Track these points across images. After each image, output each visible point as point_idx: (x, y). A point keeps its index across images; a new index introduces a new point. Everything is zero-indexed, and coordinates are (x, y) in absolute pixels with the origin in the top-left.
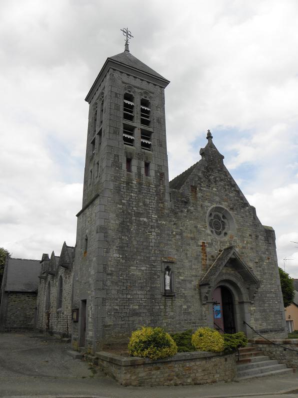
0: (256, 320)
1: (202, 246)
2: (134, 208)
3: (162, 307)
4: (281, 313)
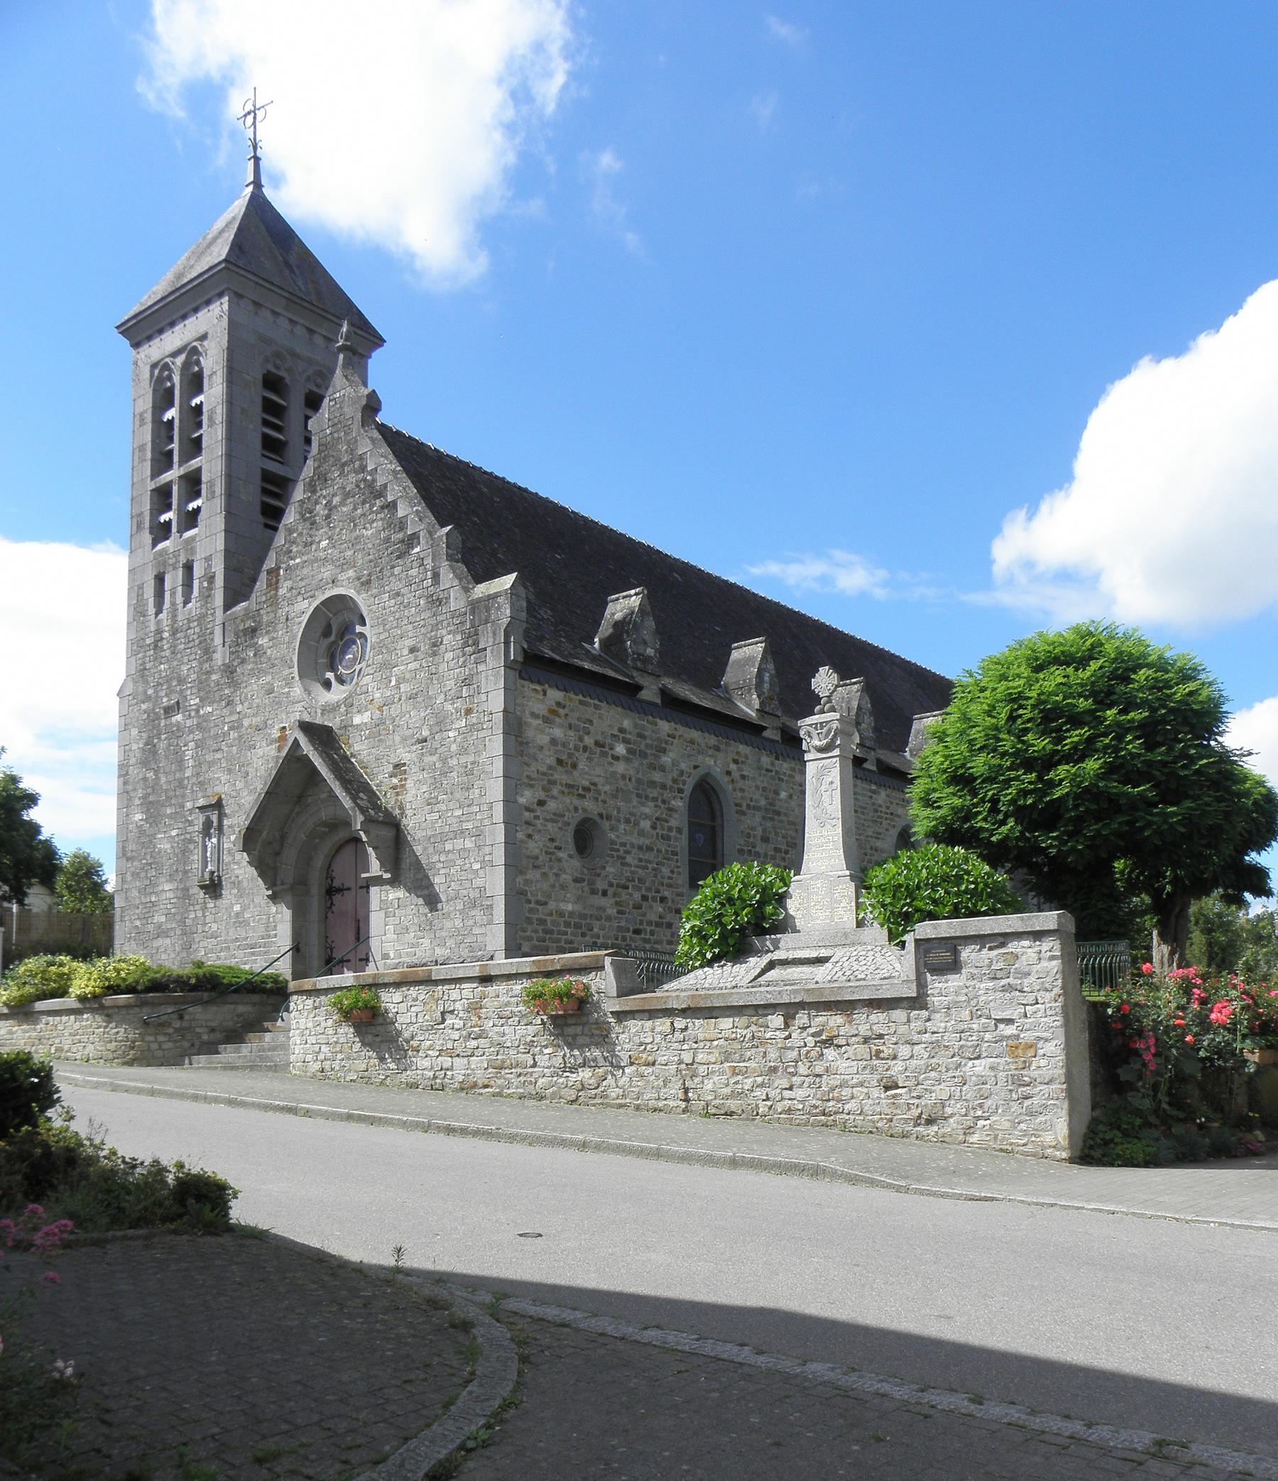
0: (402, 930)
3: (200, 914)
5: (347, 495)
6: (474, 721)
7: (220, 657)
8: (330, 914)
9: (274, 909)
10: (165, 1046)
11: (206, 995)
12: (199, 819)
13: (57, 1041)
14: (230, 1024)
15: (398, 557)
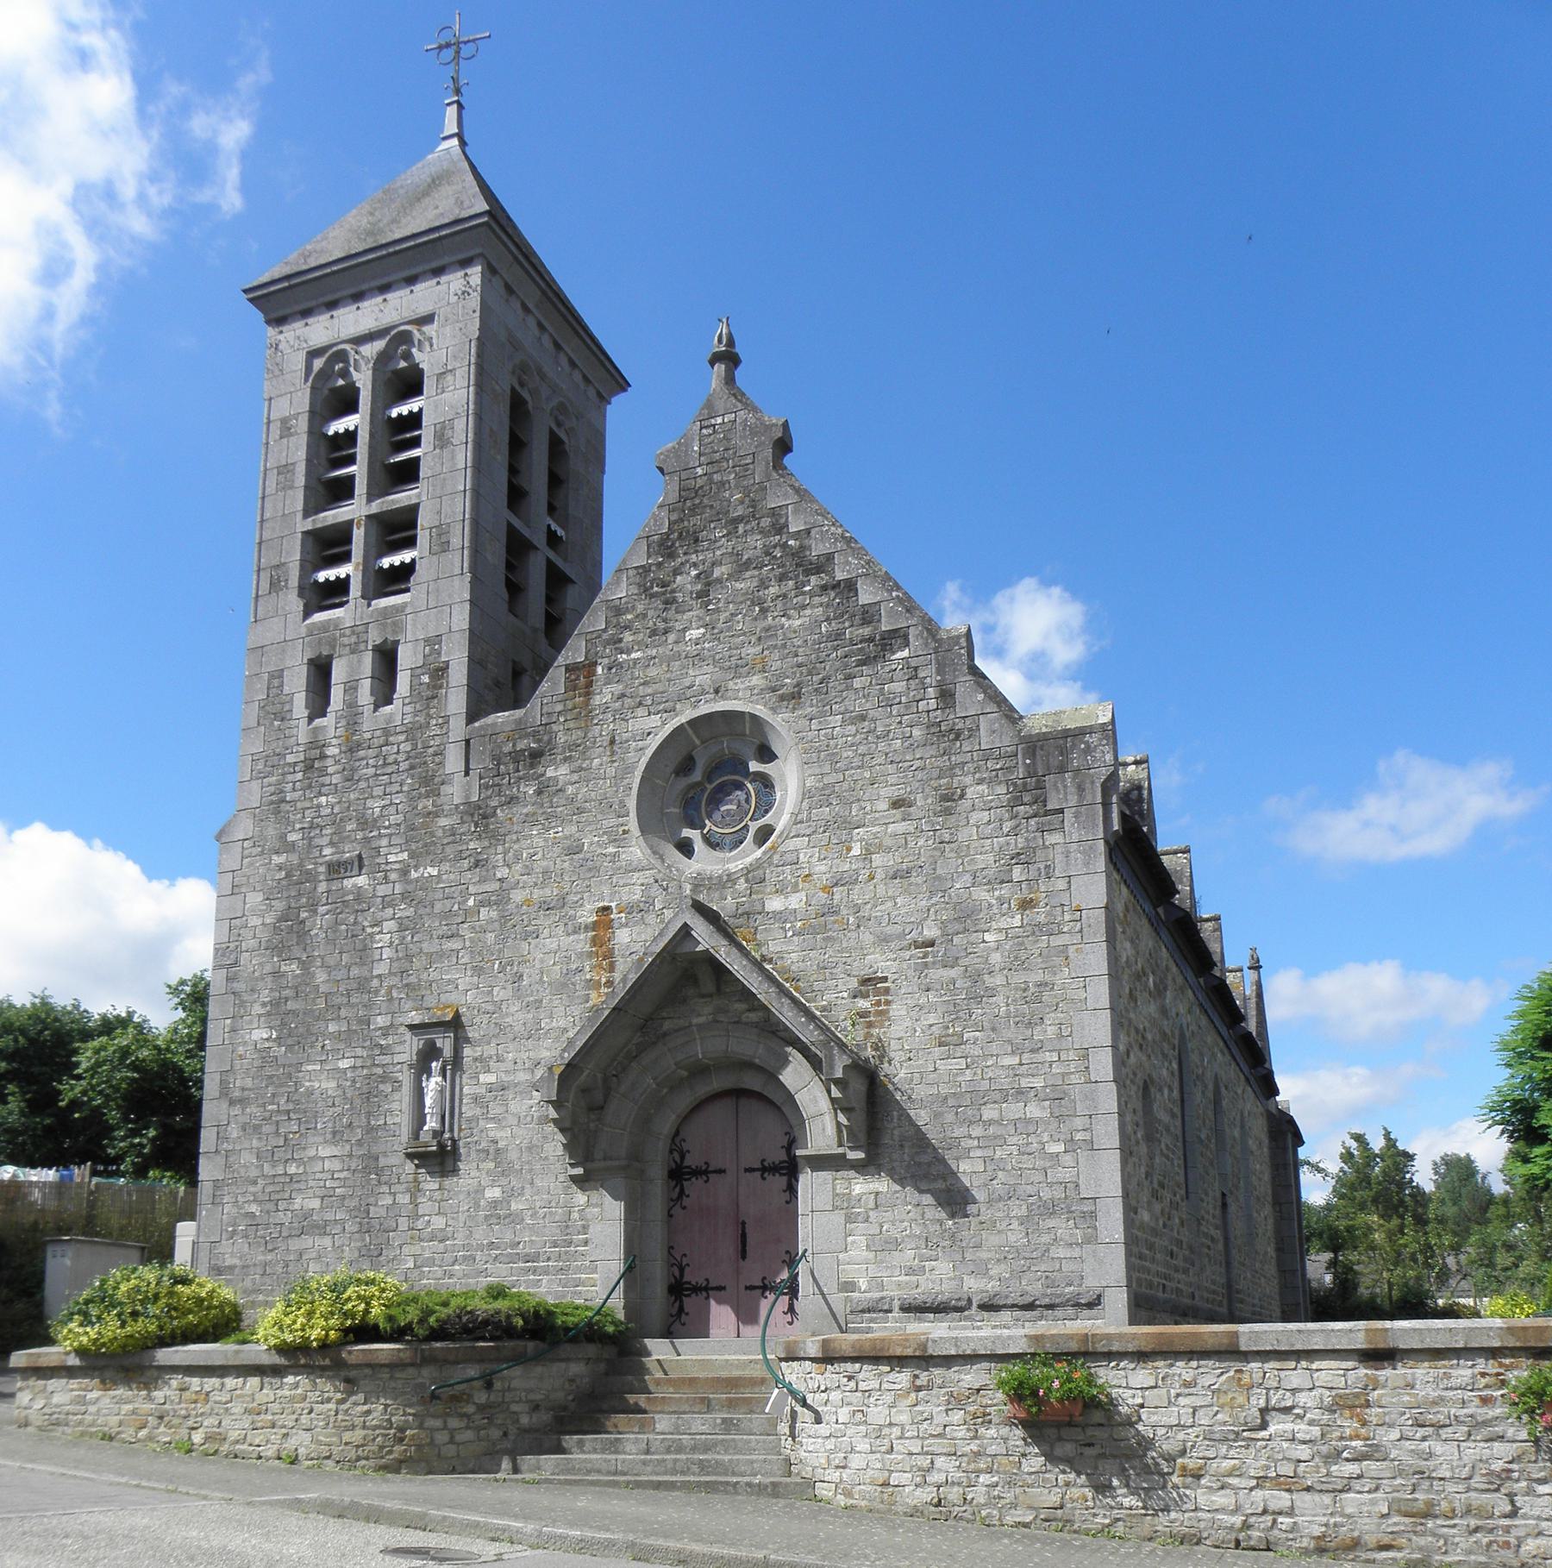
0: (884, 1246)
2: (327, 851)
3: (404, 1199)
6: (1042, 918)
7: (456, 791)
8: (677, 1210)
9: (581, 1198)
10: (459, 1438)
11: (531, 1346)
12: (409, 1048)
13: (213, 1421)
14: (560, 1395)
15: (861, 663)
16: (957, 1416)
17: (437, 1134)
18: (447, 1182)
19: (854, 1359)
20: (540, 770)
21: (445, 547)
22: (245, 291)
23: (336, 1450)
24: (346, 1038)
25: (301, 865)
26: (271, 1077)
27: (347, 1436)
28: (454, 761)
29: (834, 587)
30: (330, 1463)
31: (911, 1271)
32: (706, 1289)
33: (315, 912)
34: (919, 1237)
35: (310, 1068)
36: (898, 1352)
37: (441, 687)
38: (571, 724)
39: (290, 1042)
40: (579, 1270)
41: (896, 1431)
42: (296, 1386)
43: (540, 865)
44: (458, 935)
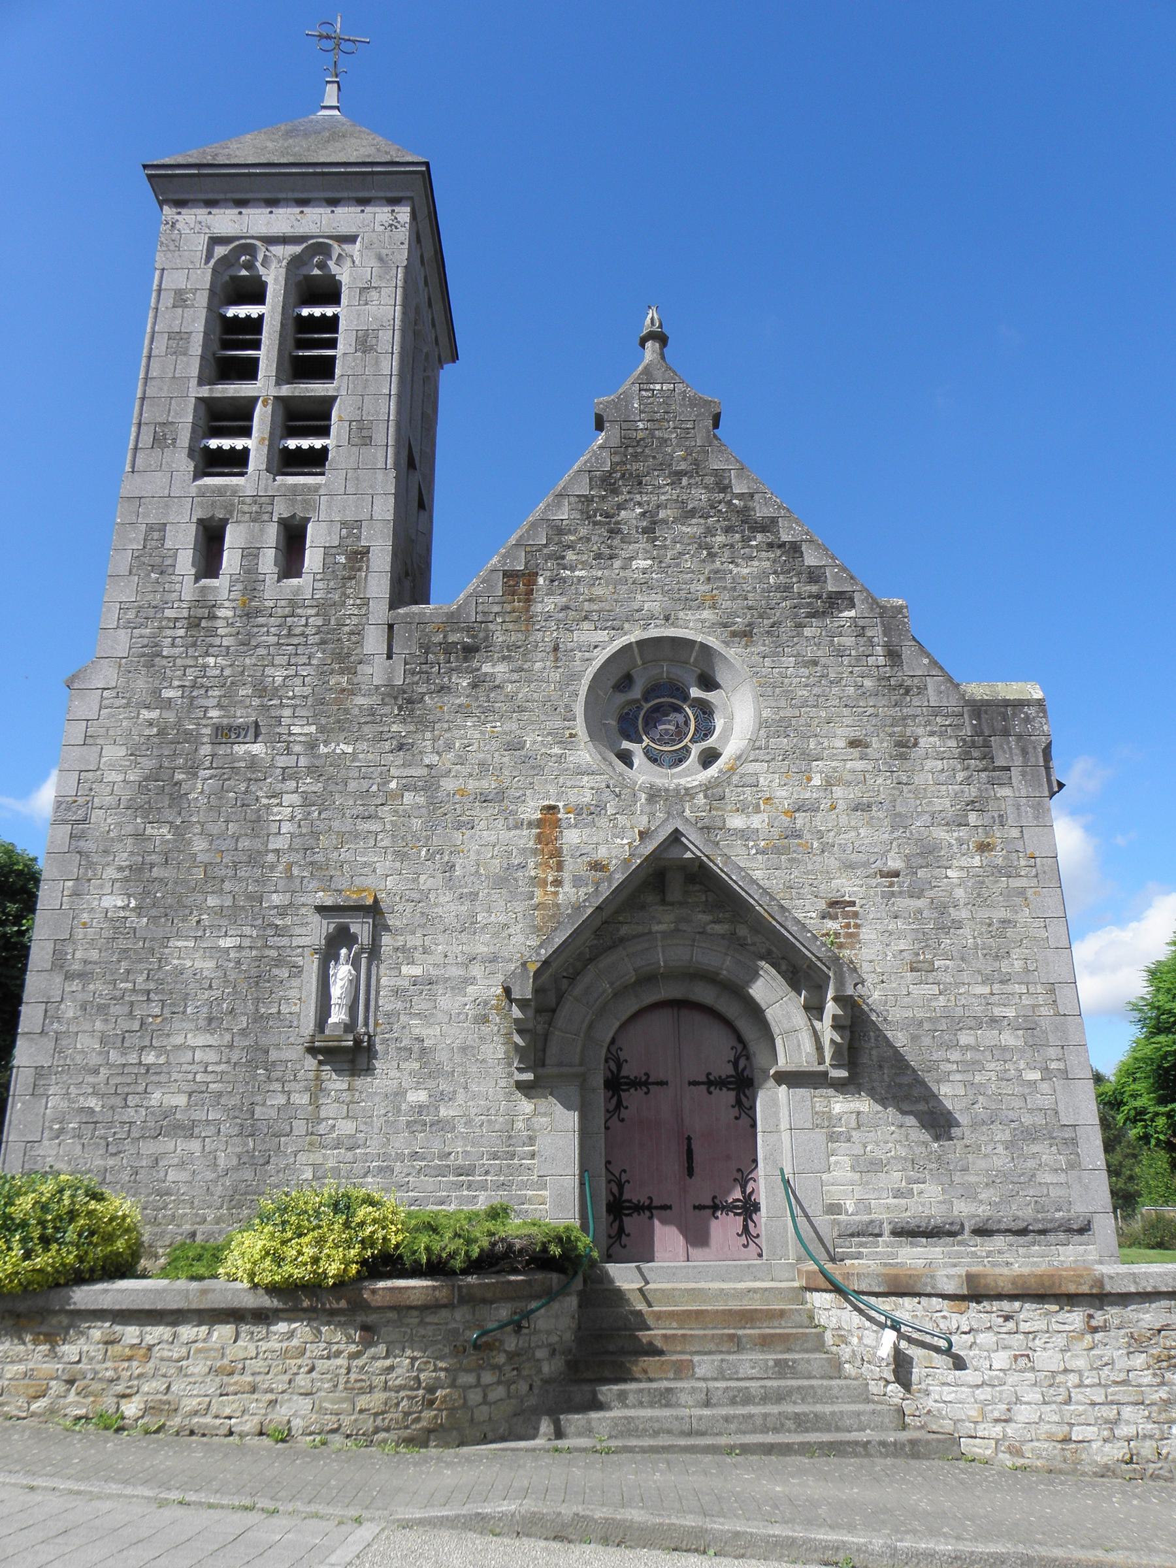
0: (869, 1167)
1: (539, 823)
2: (213, 713)
3: (301, 1099)
4: (1068, 1134)
5: (688, 514)
6: (1000, 861)
7: (376, 671)
9: (526, 1106)
12: (316, 930)
13: (158, 1385)
16: (1140, 1360)
17: (350, 1027)
18: (359, 1082)
19: (1013, 1297)
20: (475, 664)
21: (367, 441)
22: (145, 167)
23: (346, 1421)
24: (231, 914)
25: (179, 724)
26: (126, 951)
27: (363, 1402)
28: (374, 642)
29: (780, 546)
30: (337, 1440)
31: (899, 1194)
32: (650, 1208)
33: (195, 775)
34: (905, 1159)
35: (180, 944)
36: (1072, 1289)
37: (360, 570)
38: (511, 626)
39: (154, 912)
40: (524, 1185)
41: (1073, 1379)
42: (291, 1334)
43: (475, 757)
44: (376, 817)
